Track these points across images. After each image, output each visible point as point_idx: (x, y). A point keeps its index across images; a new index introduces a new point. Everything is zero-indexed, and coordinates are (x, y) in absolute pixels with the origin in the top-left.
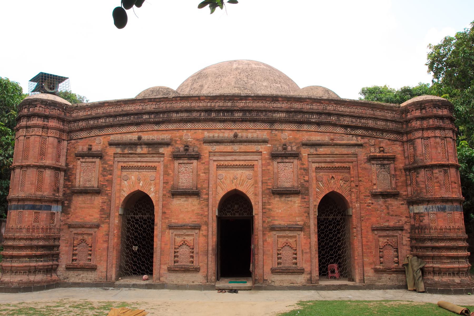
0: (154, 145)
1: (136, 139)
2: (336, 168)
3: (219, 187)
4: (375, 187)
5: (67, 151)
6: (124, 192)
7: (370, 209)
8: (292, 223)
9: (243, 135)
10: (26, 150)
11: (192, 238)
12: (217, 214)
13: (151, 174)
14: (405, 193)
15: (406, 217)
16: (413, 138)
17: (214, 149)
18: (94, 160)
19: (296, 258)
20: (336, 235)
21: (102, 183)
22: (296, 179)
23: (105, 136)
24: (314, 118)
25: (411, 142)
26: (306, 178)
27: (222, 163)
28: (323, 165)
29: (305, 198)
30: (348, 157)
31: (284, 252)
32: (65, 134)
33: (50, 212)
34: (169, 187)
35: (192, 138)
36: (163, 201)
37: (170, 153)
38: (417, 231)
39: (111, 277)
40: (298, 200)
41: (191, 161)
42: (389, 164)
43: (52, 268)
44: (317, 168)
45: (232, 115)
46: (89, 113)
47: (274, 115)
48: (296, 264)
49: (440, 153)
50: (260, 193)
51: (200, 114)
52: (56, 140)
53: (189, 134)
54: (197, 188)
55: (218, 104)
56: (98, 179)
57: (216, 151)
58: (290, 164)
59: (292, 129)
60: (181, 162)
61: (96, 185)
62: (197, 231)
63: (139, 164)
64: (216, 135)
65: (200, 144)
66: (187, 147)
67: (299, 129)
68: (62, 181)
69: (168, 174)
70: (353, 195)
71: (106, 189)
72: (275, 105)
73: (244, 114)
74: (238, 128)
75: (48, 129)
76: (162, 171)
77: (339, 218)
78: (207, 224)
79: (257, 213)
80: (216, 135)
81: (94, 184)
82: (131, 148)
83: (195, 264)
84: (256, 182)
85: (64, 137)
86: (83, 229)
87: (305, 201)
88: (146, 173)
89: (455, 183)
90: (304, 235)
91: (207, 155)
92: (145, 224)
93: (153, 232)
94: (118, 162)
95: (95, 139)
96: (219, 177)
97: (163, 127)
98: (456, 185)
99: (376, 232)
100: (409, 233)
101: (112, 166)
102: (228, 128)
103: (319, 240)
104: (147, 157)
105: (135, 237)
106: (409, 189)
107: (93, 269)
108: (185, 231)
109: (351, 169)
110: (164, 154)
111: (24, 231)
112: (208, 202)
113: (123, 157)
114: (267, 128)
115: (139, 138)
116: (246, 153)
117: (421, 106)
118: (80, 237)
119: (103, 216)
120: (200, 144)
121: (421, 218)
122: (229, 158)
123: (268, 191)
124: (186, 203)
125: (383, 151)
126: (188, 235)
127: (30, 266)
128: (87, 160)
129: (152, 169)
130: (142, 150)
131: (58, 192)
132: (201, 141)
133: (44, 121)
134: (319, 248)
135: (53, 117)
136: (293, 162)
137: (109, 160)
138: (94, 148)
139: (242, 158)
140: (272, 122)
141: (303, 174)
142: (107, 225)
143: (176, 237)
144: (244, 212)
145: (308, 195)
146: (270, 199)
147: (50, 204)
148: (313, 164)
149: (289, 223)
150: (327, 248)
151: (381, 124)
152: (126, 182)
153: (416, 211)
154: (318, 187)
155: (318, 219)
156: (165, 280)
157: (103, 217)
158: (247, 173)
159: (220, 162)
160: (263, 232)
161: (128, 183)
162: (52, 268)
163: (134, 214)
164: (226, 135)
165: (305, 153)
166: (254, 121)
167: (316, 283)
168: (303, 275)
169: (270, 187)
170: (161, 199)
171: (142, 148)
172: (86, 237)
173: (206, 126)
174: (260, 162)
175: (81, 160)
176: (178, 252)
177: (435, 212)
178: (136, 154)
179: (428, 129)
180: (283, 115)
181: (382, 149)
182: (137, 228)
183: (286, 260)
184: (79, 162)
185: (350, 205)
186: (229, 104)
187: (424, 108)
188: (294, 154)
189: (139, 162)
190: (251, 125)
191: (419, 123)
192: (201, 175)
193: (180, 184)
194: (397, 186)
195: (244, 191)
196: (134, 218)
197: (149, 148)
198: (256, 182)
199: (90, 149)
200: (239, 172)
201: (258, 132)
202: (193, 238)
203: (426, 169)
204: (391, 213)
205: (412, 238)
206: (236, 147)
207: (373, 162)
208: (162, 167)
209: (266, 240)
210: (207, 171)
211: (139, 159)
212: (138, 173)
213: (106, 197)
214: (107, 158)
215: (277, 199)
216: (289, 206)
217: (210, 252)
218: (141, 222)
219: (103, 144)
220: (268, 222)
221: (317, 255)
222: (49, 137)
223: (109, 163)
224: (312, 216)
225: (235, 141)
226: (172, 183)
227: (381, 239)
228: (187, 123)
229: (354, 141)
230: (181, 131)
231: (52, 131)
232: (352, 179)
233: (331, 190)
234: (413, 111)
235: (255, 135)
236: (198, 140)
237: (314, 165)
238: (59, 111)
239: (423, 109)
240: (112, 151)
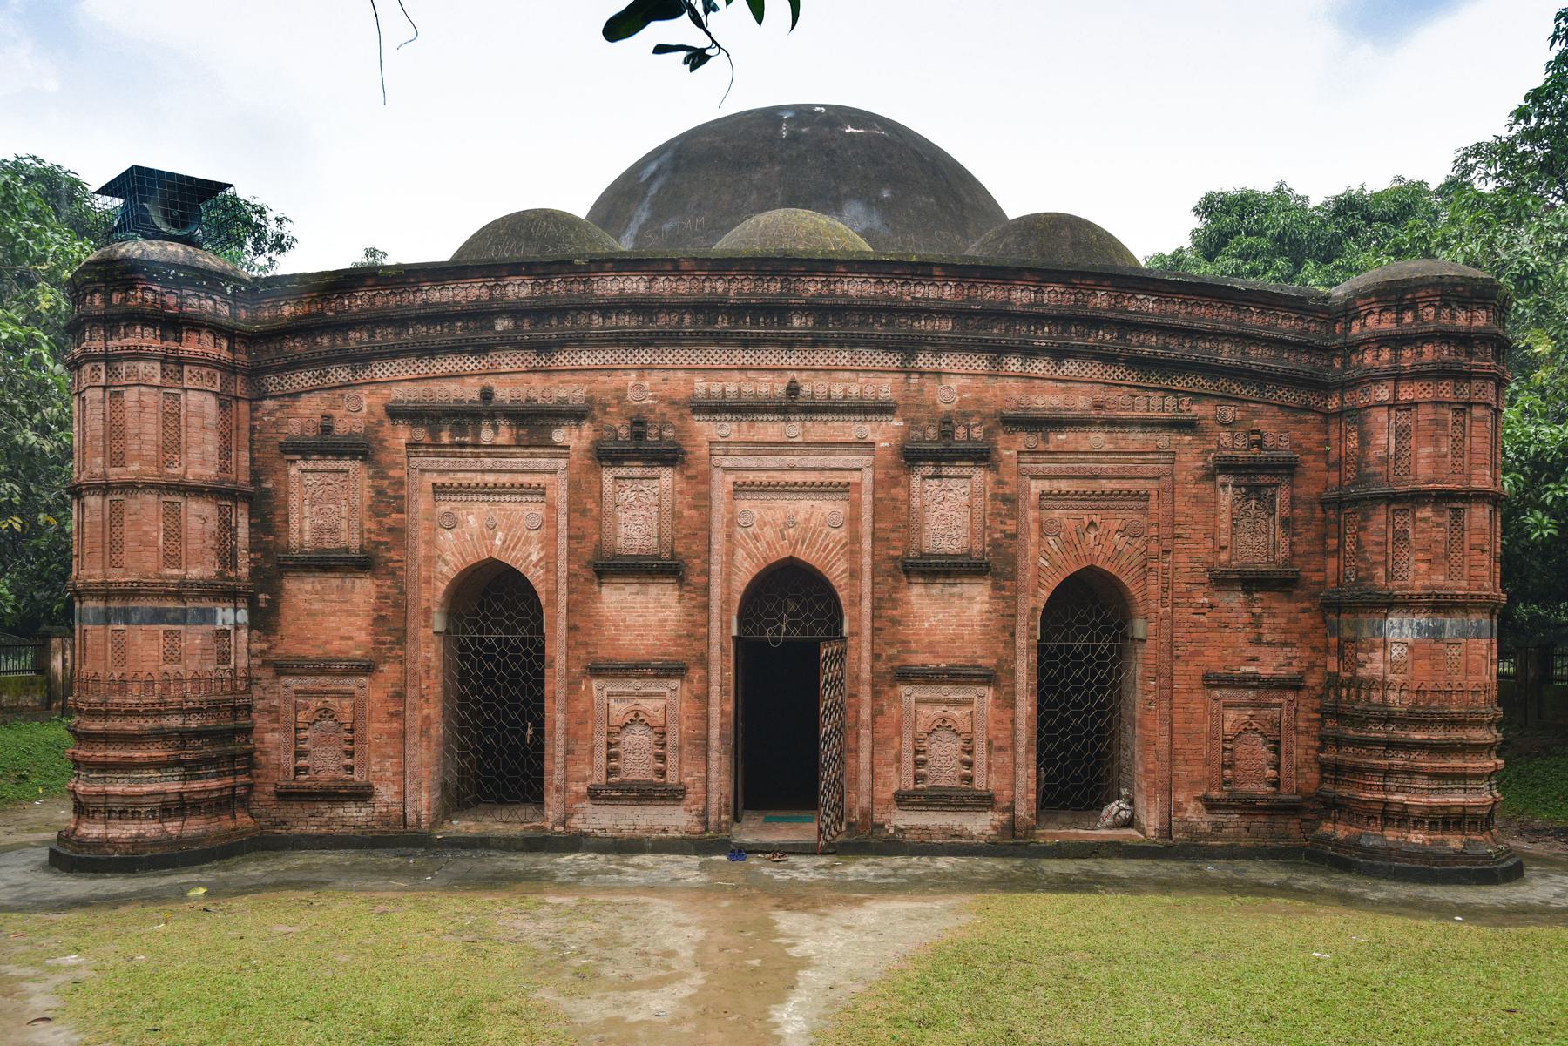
0: (533, 422)
1: (477, 397)
2: (1104, 496)
3: (740, 553)
4: (1223, 557)
5: (252, 434)
6: (447, 564)
7: (1202, 625)
8: (961, 661)
9: (815, 386)
10: (115, 432)
11: (659, 703)
12: (735, 633)
14: (1316, 577)
15: (1314, 649)
17: (724, 432)
18: (342, 464)
19: (970, 764)
20: (1094, 698)
22: (978, 528)
23: (374, 387)
24: (1044, 336)
25: (1356, 415)
26: (1010, 526)
27: (750, 476)
28: (1064, 486)
29: (1003, 588)
30: (1146, 462)
31: (934, 746)
32: (239, 378)
33: (212, 628)
34: (587, 550)
35: (653, 397)
36: (570, 593)
38: (1344, 692)
39: (419, 820)
40: (981, 594)
41: (655, 472)
42: (1277, 485)
43: (233, 795)
44: (1043, 495)
45: (784, 322)
47: (916, 324)
48: (969, 779)
49: (1445, 456)
50: (867, 569)
51: (681, 320)
52: (211, 402)
53: (647, 384)
54: (673, 556)
55: (735, 288)
56: (361, 524)
57: (733, 437)
58: (960, 482)
59: (971, 370)
60: (623, 472)
61: (355, 543)
62: (675, 683)
63: (490, 478)
64: (732, 388)
65: (681, 417)
66: (639, 424)
67: (994, 371)
68: (243, 533)
69: (584, 513)
70: (1152, 578)
71: (387, 555)
72: (920, 292)
73: (821, 322)
74: (801, 366)
75: (182, 365)
76: (565, 499)
77: (1104, 645)
78: (704, 662)
79: (855, 630)
80: (733, 385)
81: (349, 539)
82: (459, 429)
84: (855, 538)
85: (239, 388)
86: (322, 679)
87: (1003, 598)
88: (512, 506)
89: (1483, 551)
90: (996, 699)
91: (704, 451)
92: (514, 659)
93: (541, 684)
94: (423, 470)
95: (342, 396)
96: (741, 521)
97: (563, 359)
98: (1486, 556)
99: (1217, 693)
100: (1320, 697)
101: (400, 483)
102: (771, 366)
103: (1039, 710)
104: (512, 455)
105: (486, 697)
106: (1332, 564)
107: (363, 794)
108: (637, 683)
109: (1153, 499)
110: (567, 447)
111: (136, 689)
112: (708, 595)
113: (438, 455)
114: (893, 367)
115: (487, 394)
116: (826, 446)
117: (1401, 299)
118: (315, 703)
120: (681, 417)
121: (1360, 656)
122: (771, 461)
123: (889, 565)
124: (641, 598)
125: (1259, 444)
126: (647, 695)
127: (164, 793)
129: (532, 495)
130: (496, 434)
131: (235, 566)
132: (685, 407)
133: (164, 338)
134: (1039, 734)
135: (196, 324)
136: (970, 477)
137: (394, 465)
138: (341, 428)
139: (812, 461)
140: (908, 347)
141: (1000, 515)
142: (397, 666)
143: (612, 702)
144: (817, 624)
145: (1012, 577)
146: (895, 589)
147: (211, 604)
148: (1033, 483)
149: (953, 661)
150: (1064, 735)
151: (1258, 357)
152: (449, 535)
154: (1044, 553)
155: (1042, 649)
156: (580, 826)
157: (384, 643)
158: (831, 508)
159: (745, 474)
160: (873, 685)
161: (457, 536)
162: (233, 795)
163: (480, 631)
164: (764, 389)
165: (1008, 449)
166: (851, 343)
167: (1026, 837)
168: (990, 815)
169: (896, 553)
170: (563, 588)
171: (495, 428)
173: (699, 357)
174: (868, 476)
175: (302, 464)
176: (618, 743)
177: (1409, 640)
178: (477, 446)
179: (1417, 375)
180: (945, 325)
181: (1257, 437)
182: (492, 673)
183: (940, 770)
184: (293, 471)
185: (1141, 609)
186: (775, 287)
187: (1412, 306)
188: (976, 451)
189: (490, 471)
190: (843, 357)
191: (1386, 354)
192: (686, 513)
193: (620, 542)
194: (1294, 555)
195: (817, 564)
196: (482, 641)
197: (519, 427)
198: (855, 538)
199: (327, 430)
200: (802, 507)
201: (862, 378)
202: (663, 703)
203: (1394, 506)
204: (1268, 637)
205: (1324, 714)
206: (794, 429)
207: (1221, 478)
208: (563, 489)
209: (882, 713)
210: (703, 501)
211: (488, 462)
212: (485, 506)
213: (388, 582)
214: (384, 457)
216: (953, 612)
217: (715, 742)
218: (502, 654)
219: (371, 413)
220: (891, 658)
221: (1033, 757)
222: (186, 390)
223: (391, 473)
224: (1022, 642)
225: (791, 405)
226: (596, 537)
227: (1231, 715)
228: (636, 347)
230: (620, 373)
231: (195, 370)
232: (1153, 531)
233: (1085, 565)
234: (1371, 313)
235: (854, 390)
236: (673, 403)
237: (1036, 487)
238: (210, 303)
239: (1408, 308)
240: (401, 435)
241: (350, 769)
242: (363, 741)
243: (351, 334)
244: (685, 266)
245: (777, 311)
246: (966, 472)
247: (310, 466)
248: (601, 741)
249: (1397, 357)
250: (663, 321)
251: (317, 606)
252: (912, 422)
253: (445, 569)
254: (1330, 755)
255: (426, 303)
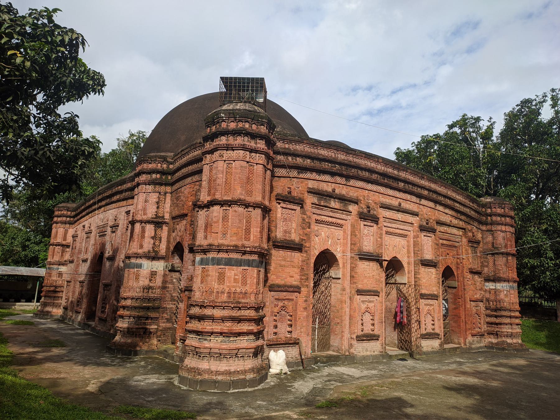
13: (338, 233)
16: (493, 229)
18: (294, 207)
21: (302, 238)
28: (445, 242)
34: (356, 248)
37: (357, 213)
41: (372, 224)
46: (287, 146)
48: (433, 329)
60: (366, 223)
63: (330, 220)
69: (356, 235)
81: (295, 237)
83: (376, 332)
97: (352, 182)
104: (337, 213)
113: (318, 209)
115: (334, 190)
118: (281, 304)
119: (303, 277)
122: (394, 225)
126: (370, 302)
128: (289, 206)
140: (420, 196)
152: (317, 238)
153: (492, 287)
156: (354, 352)
157: (303, 279)
170: (349, 261)
172: (286, 302)
190: (408, 197)
193: (364, 247)
199: (290, 193)
205: (487, 309)
211: (331, 214)
215: (423, 269)
225: (399, 209)
229: (461, 224)
236: (375, 203)
237: (441, 241)
240: (310, 200)
241: (290, 332)
242: (296, 320)
243: (298, 159)
244: (380, 161)
245: (397, 179)
246: (431, 235)
247: (284, 206)
248: (359, 318)
249: (487, 219)
250: (374, 176)
251: (283, 263)
252: (421, 220)
253: (315, 251)
254: (489, 319)
255: (318, 153)
